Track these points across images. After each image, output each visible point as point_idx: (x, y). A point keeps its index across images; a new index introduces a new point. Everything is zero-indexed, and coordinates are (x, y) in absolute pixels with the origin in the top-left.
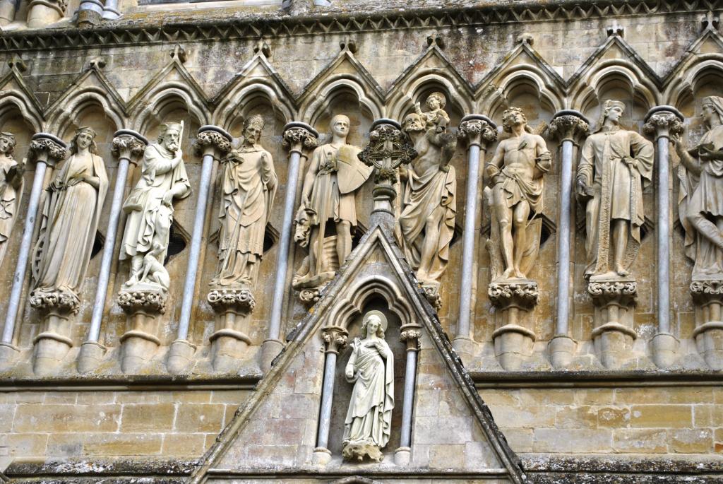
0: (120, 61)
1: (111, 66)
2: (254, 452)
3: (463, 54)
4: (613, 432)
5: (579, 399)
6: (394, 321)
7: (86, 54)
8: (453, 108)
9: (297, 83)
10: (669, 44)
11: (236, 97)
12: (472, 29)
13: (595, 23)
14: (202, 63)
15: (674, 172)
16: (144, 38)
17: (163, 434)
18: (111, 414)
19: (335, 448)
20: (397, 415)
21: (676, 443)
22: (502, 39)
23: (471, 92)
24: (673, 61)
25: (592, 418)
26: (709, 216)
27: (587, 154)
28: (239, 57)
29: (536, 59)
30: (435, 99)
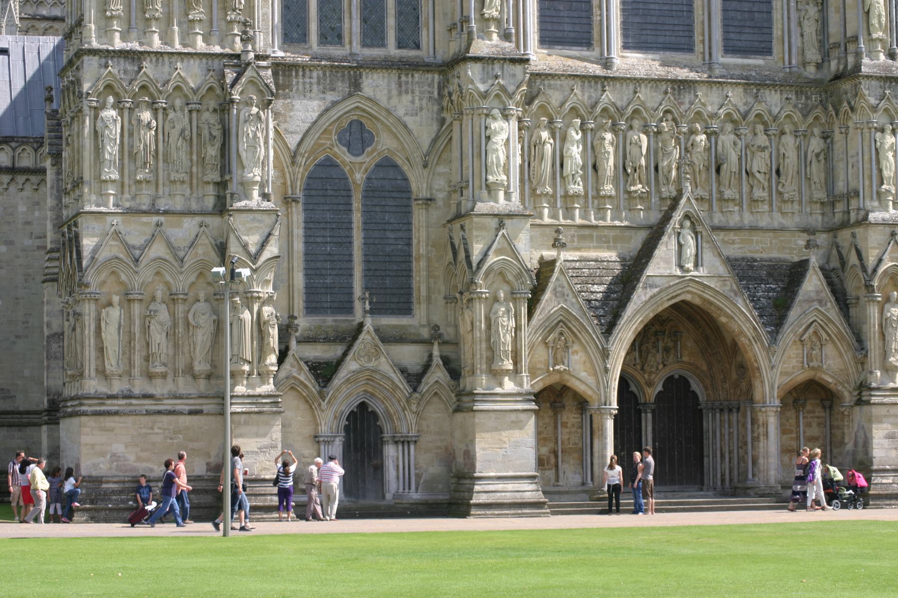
0: (550, 86)
1: (550, 92)
2: (659, 268)
3: (677, 97)
4: (732, 246)
5: (722, 234)
6: (692, 223)
7: (535, 83)
8: (674, 120)
9: (619, 104)
10: (745, 101)
11: (598, 109)
12: (679, 87)
13: (721, 88)
14: (582, 91)
15: (746, 151)
16: (559, 78)
17: (592, 245)
18: (573, 236)
19: (681, 267)
20: (697, 255)
21: (750, 251)
22: (690, 92)
23: (682, 116)
24: (746, 108)
25: (726, 242)
26: (759, 172)
27: (720, 143)
28: (595, 90)
29: (704, 105)
30: (670, 117)
